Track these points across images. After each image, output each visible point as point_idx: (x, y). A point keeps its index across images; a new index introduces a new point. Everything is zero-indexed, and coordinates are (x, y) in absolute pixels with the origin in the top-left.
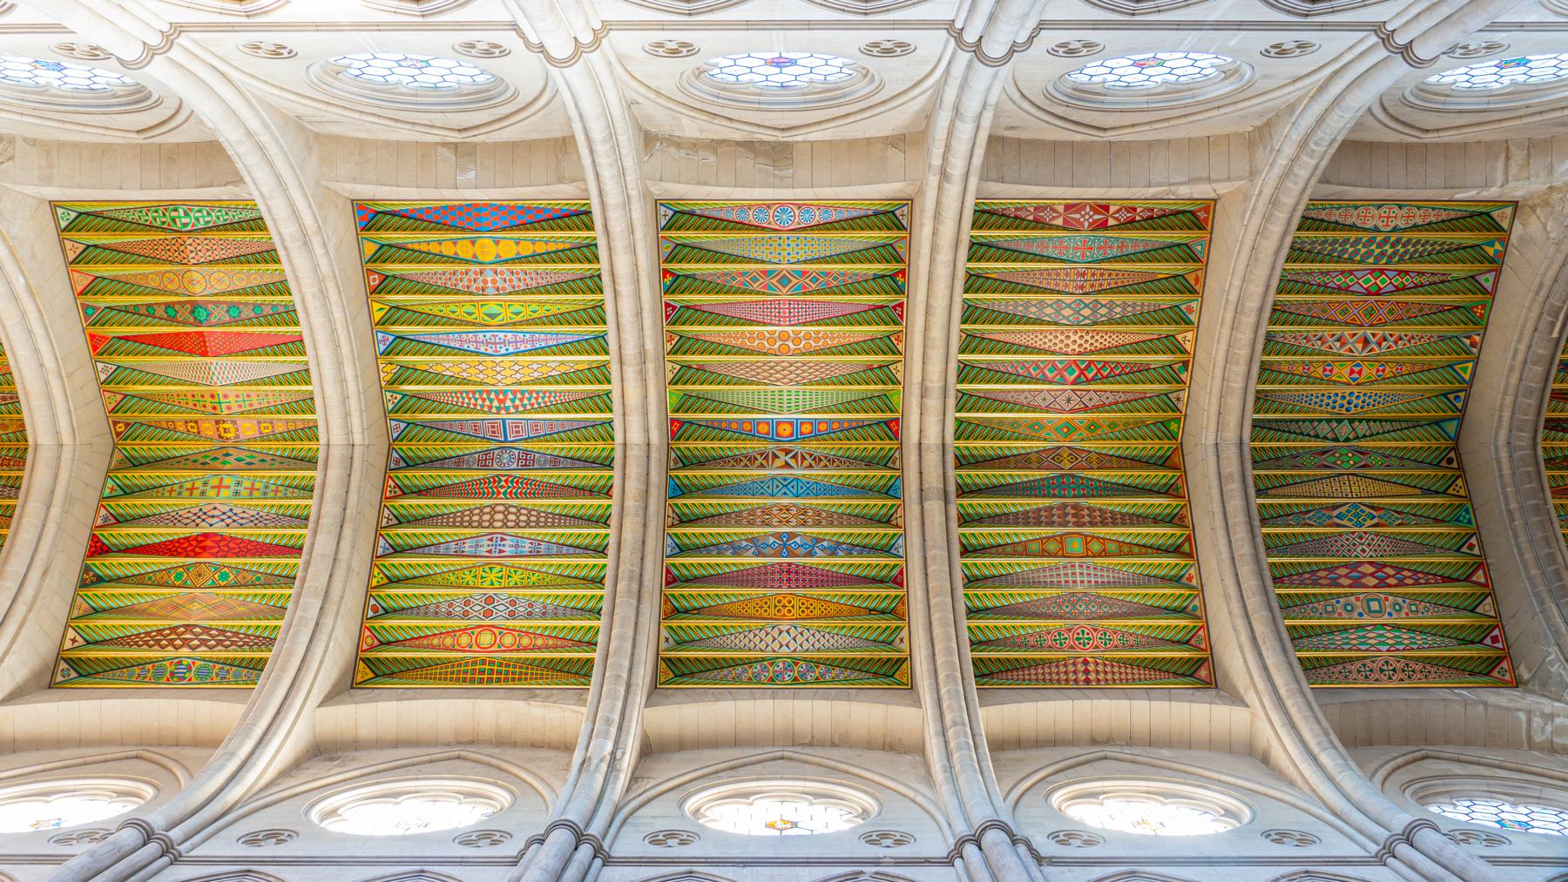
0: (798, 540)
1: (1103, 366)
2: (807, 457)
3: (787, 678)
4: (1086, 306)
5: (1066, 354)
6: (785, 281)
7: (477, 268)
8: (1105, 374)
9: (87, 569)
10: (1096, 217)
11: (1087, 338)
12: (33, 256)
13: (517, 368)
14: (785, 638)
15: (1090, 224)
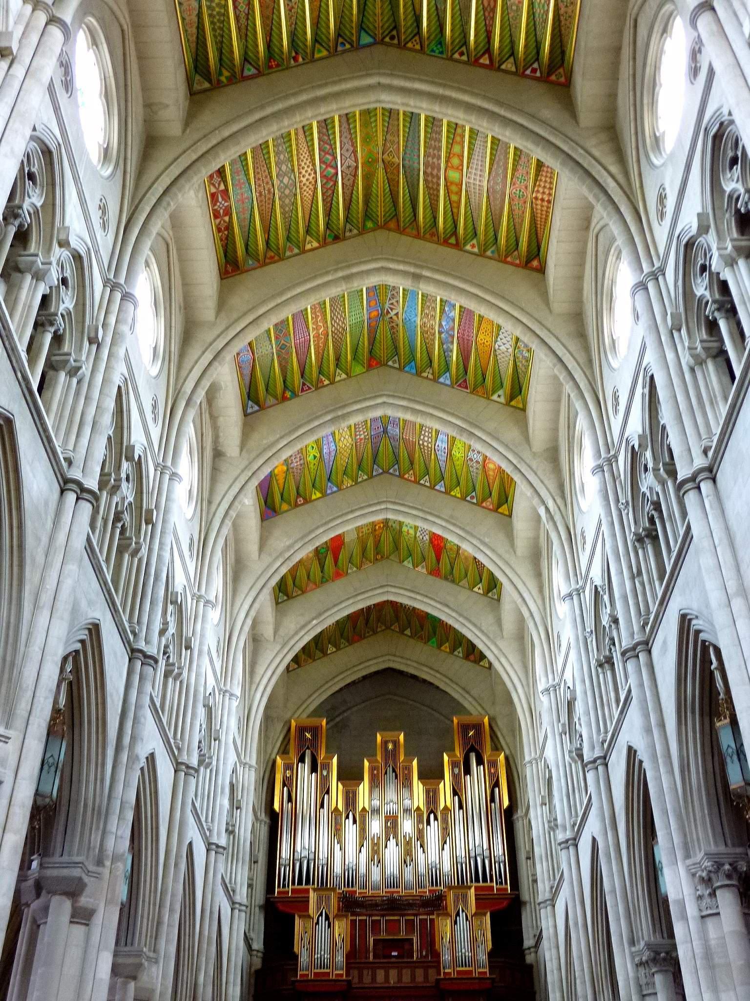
0: (444, 323)
1: (323, 151)
2: (391, 302)
3: (527, 355)
4: (281, 182)
5: (316, 181)
6: (283, 347)
7: (291, 470)
8: (328, 147)
9: (446, 579)
10: (220, 199)
11: (303, 172)
12: (302, 615)
13: (342, 439)
14: (503, 348)
15: (226, 201)
